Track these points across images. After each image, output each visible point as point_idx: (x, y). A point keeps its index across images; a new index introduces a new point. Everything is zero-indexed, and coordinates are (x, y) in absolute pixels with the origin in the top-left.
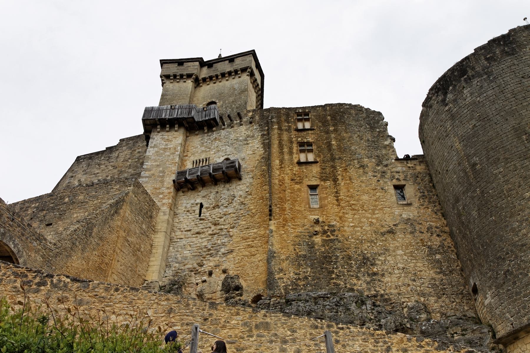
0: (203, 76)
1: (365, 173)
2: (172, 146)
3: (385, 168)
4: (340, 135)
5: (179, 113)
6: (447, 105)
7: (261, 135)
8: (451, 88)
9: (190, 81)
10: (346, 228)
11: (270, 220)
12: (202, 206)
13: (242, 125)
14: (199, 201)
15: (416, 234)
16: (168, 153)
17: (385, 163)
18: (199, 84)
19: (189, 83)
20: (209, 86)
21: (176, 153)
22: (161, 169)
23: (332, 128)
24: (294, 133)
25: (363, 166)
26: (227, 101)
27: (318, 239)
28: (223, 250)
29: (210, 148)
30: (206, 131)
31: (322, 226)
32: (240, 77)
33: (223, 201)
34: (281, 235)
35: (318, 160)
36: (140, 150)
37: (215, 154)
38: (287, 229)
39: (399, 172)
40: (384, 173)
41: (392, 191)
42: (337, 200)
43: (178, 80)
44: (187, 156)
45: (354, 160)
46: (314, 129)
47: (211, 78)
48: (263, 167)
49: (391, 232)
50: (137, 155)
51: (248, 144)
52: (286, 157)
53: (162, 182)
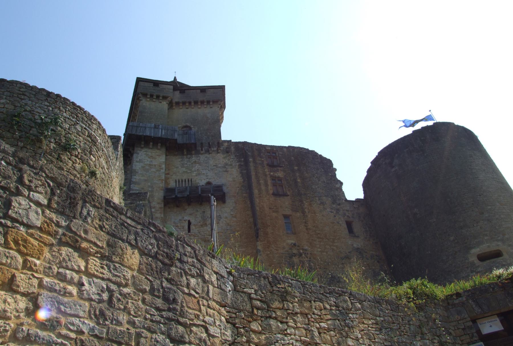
0: (177, 100)
1: (325, 209)
2: (156, 163)
3: (339, 207)
5: (163, 133)
6: (393, 167)
7: (239, 165)
8: (396, 155)
9: (165, 103)
10: (315, 252)
11: (257, 241)
12: (189, 223)
13: (218, 153)
14: (187, 218)
17: (338, 202)
18: (172, 106)
19: (164, 105)
20: (181, 110)
21: (162, 170)
22: (149, 184)
23: (296, 168)
25: (322, 203)
26: (202, 128)
29: (191, 170)
30: (185, 153)
31: (298, 250)
32: (211, 108)
34: (267, 255)
35: (289, 193)
37: (196, 176)
38: (271, 250)
39: (348, 211)
40: (338, 210)
41: (345, 226)
42: (307, 229)
43: (154, 100)
44: (168, 174)
45: (315, 197)
46: (282, 167)
47: (184, 103)
48: (244, 195)
49: (348, 257)
51: (226, 171)
52: (263, 188)
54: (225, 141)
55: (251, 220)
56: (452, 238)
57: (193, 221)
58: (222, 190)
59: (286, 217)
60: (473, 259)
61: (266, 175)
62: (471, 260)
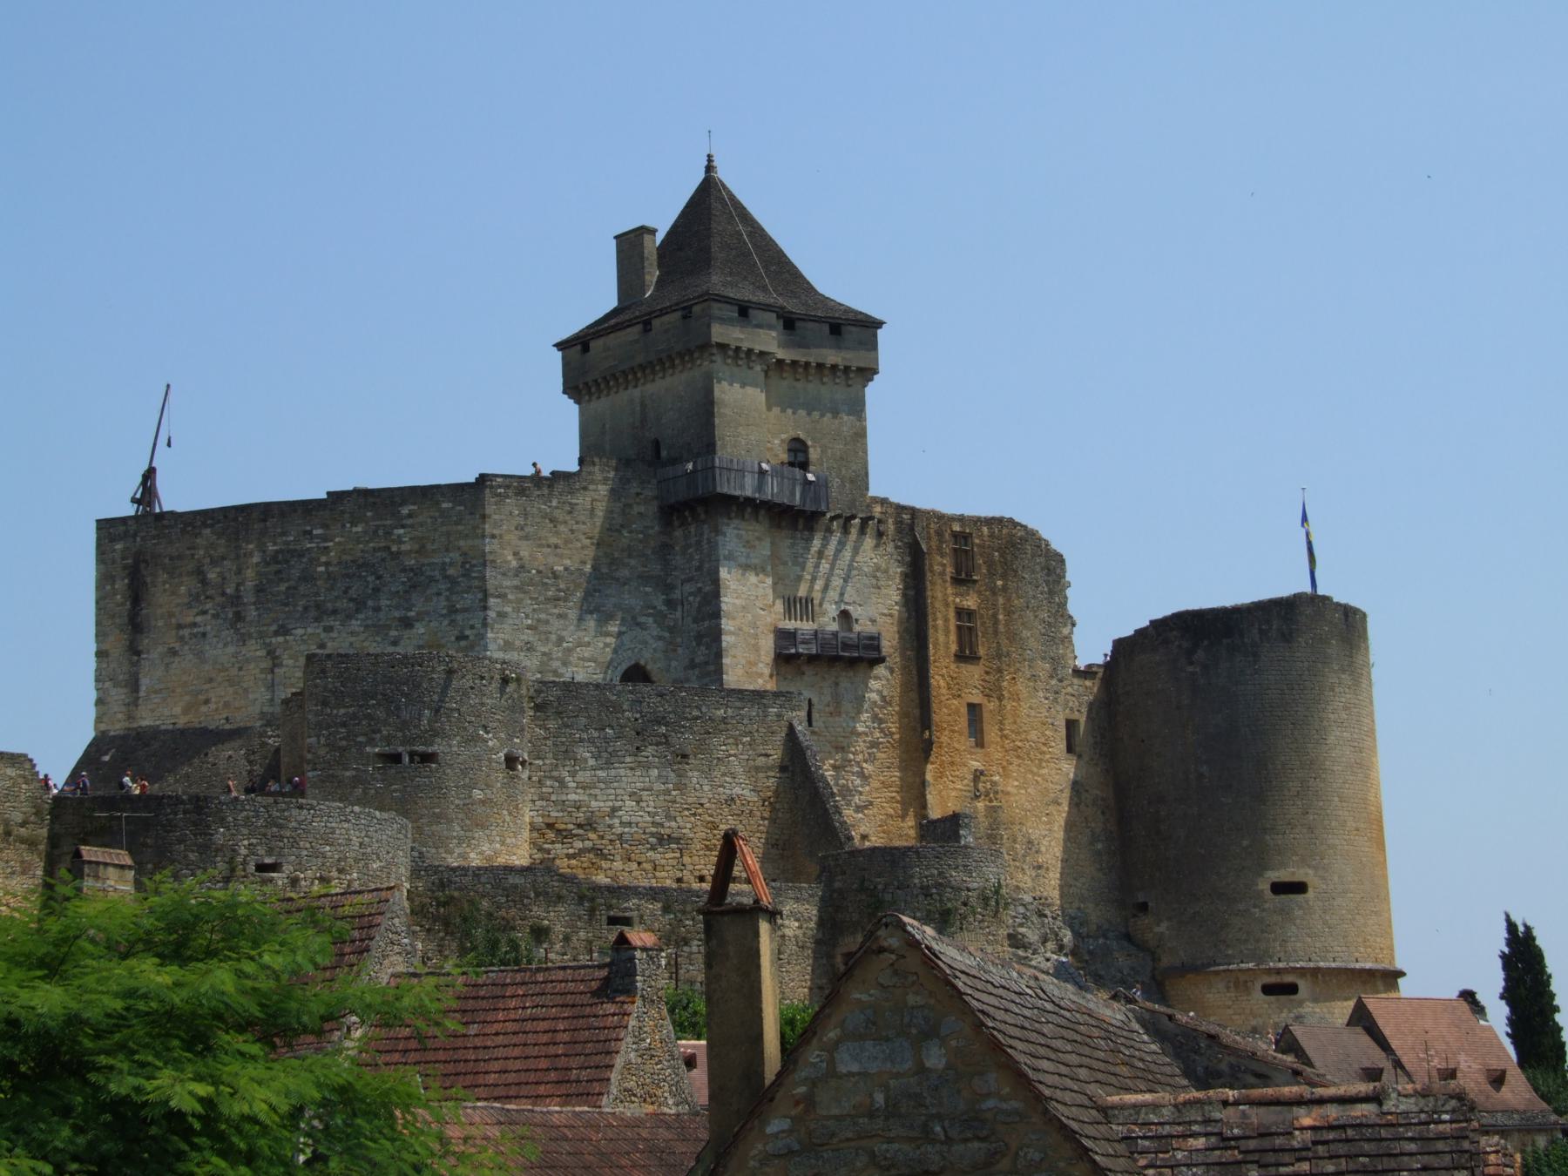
4: (1009, 600)
15: (1082, 807)
23: (1000, 583)
53: (756, 648)
54: (875, 500)
55: (917, 712)
56: (1245, 843)
57: (815, 701)
58: (878, 648)
59: (973, 709)
60: (1264, 886)
61: (947, 605)
62: (1261, 887)
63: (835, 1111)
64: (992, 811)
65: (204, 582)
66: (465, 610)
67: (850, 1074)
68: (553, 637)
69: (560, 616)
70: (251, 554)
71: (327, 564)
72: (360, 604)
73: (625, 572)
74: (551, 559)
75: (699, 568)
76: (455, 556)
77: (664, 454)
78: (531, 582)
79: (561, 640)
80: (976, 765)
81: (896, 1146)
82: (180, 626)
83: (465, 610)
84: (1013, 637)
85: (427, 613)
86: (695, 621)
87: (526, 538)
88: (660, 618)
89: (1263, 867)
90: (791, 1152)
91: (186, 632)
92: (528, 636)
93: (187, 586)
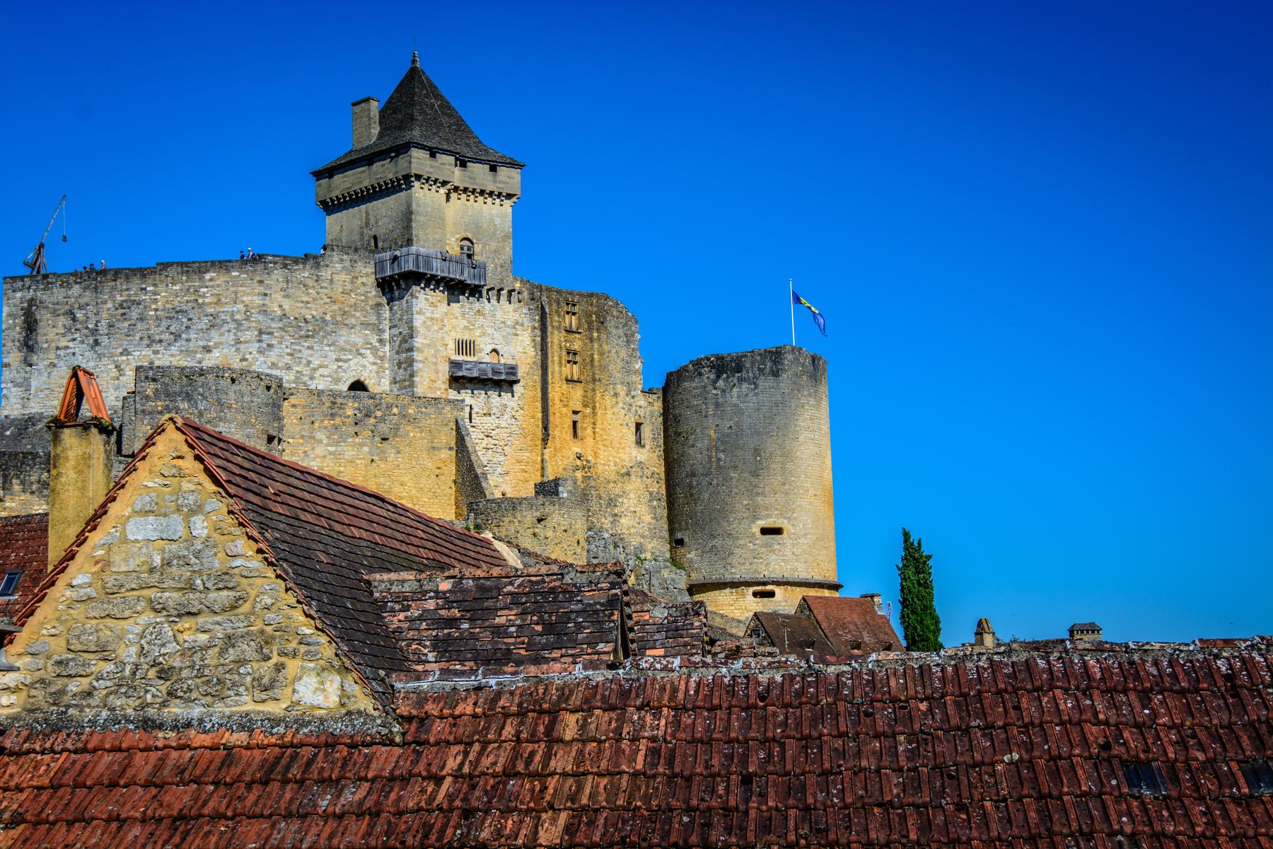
16: (435, 327)
23: (595, 335)
24: (564, 333)
27: (579, 475)
28: (499, 470)
33: (495, 410)
36: (364, 280)
49: (628, 474)
50: (362, 289)
53: (437, 372)
55: (540, 415)
58: (515, 374)
60: (756, 530)
63: (124, 569)
64: (586, 478)
65: (74, 319)
66: (246, 342)
67: (137, 541)
68: (304, 361)
69: (309, 348)
70: (105, 302)
71: (156, 310)
72: (177, 336)
73: (353, 321)
74: (303, 311)
75: (400, 320)
76: (241, 307)
77: (380, 245)
78: (290, 325)
79: (309, 363)
80: (578, 450)
81: (167, 594)
82: (58, 348)
83: (246, 342)
84: (603, 368)
85: (221, 343)
86: (398, 353)
87: (287, 296)
88: (375, 351)
89: (756, 518)
90: (90, 598)
91: (62, 353)
92: (287, 359)
93: (63, 321)
